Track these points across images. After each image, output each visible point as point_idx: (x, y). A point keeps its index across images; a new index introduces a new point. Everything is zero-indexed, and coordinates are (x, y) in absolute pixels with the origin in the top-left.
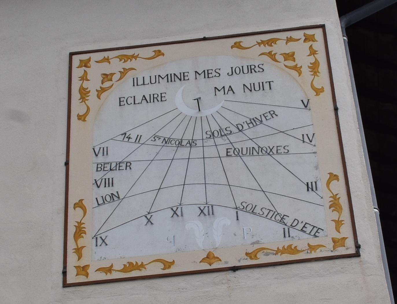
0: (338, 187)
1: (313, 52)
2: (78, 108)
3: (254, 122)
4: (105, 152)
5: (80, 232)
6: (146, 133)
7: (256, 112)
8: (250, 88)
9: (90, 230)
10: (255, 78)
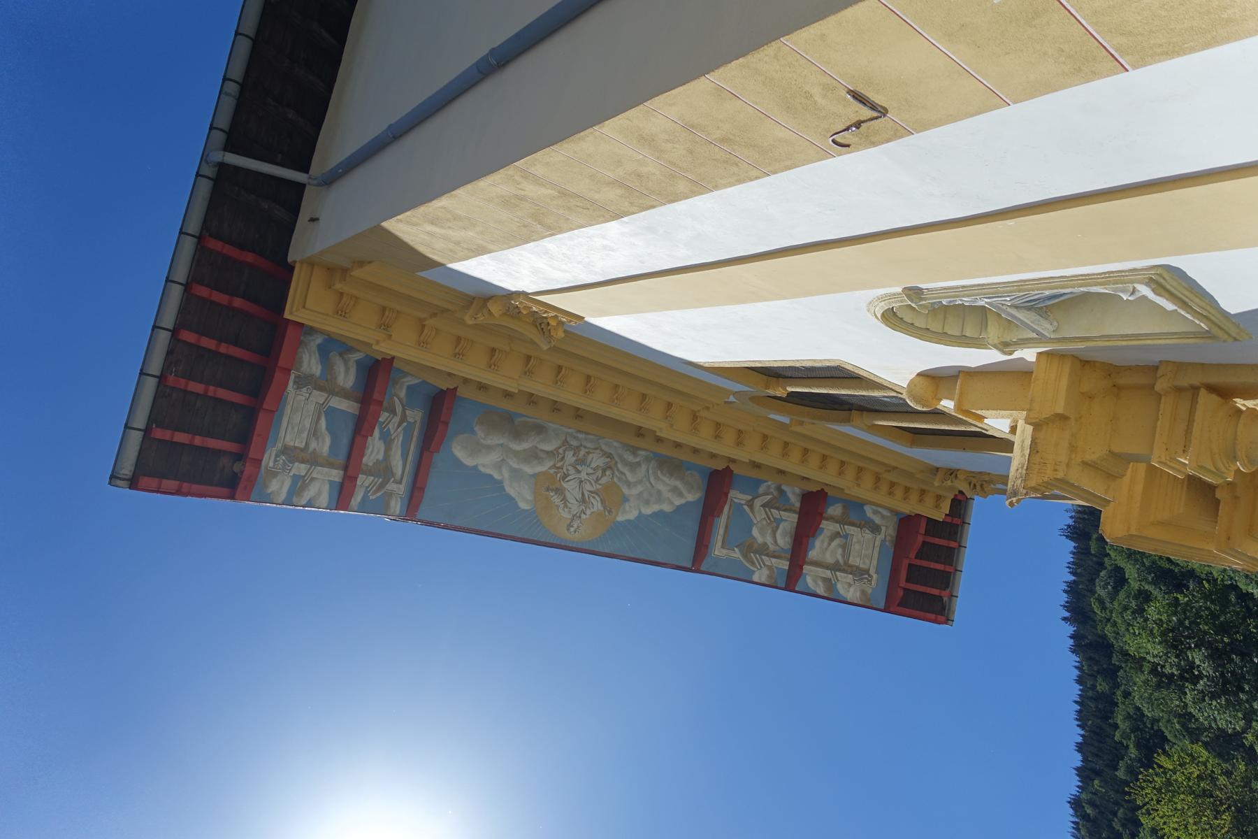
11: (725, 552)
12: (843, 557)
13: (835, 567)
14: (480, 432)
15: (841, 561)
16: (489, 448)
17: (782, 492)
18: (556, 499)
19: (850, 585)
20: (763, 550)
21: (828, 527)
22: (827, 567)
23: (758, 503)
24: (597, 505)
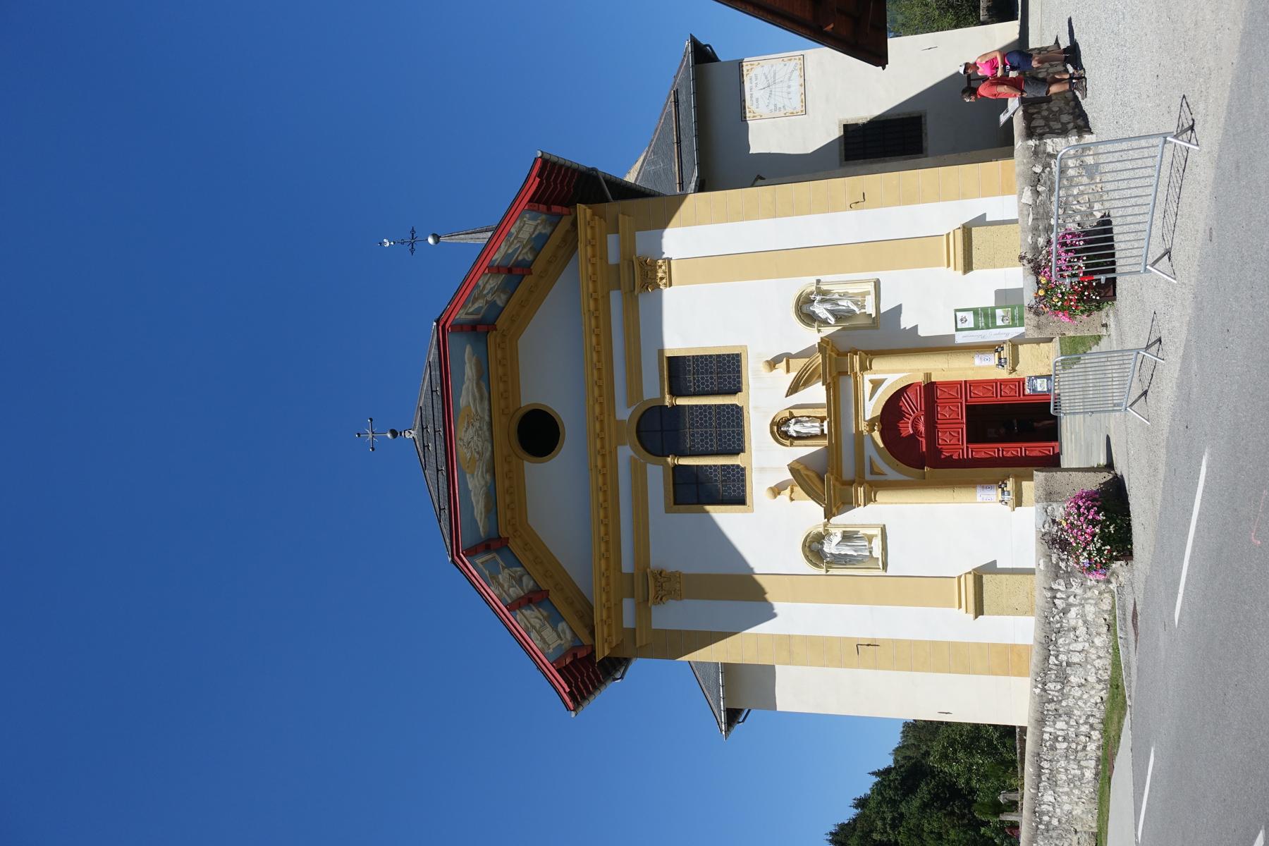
0: (785, 59)
1: (747, 65)
2: (759, 117)
3: (766, 78)
4: (771, 110)
5: (792, 113)
6: (767, 101)
7: (763, 77)
8: (756, 79)
9: (792, 111)
10: (754, 79)
11: (481, 566)
12: (540, 628)
13: (534, 627)
14: (474, 361)
15: (537, 628)
16: (471, 368)
17: (521, 577)
18: (466, 426)
19: (538, 640)
20: (502, 587)
21: (536, 613)
22: (529, 623)
23: (506, 571)
24: (468, 455)
